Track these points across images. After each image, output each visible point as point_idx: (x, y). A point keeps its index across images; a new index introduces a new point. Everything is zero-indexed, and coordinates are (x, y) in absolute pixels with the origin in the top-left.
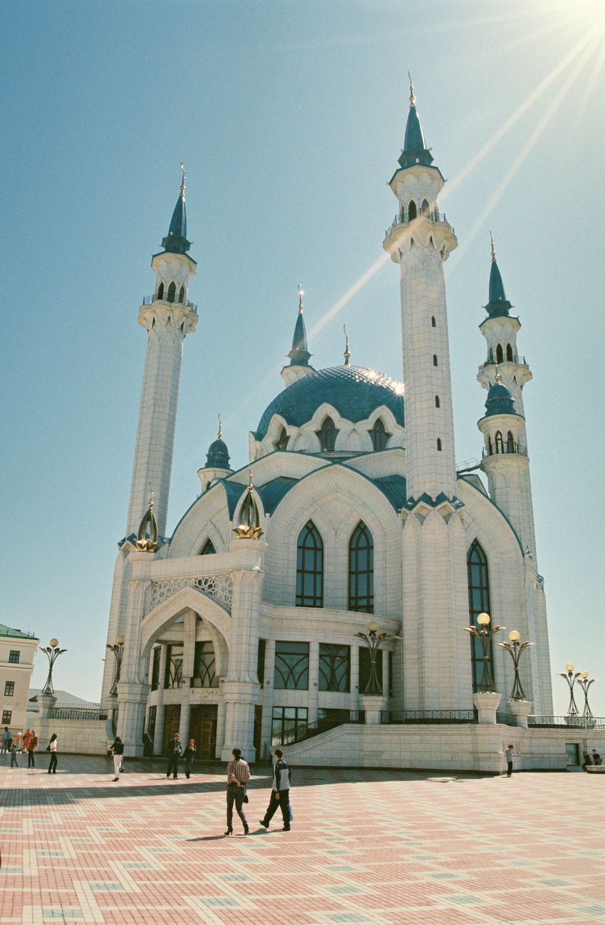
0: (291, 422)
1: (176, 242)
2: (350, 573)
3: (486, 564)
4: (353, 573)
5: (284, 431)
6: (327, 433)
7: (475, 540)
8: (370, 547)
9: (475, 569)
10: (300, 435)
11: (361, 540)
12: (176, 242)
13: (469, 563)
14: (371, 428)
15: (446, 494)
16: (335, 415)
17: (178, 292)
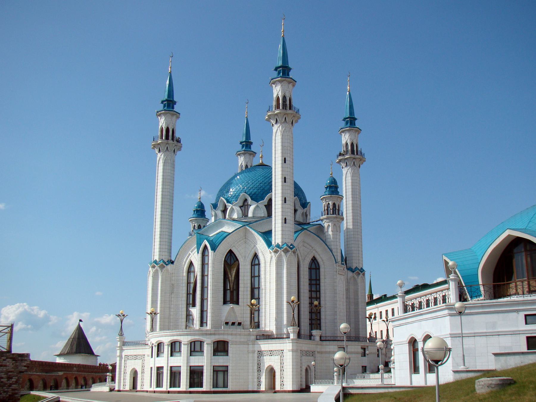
0: (228, 202)
1: (169, 104)
2: (252, 277)
3: (319, 269)
4: (253, 277)
5: (226, 206)
6: (244, 206)
7: (314, 257)
8: (259, 264)
9: (313, 271)
10: (232, 209)
11: (255, 260)
12: (169, 104)
13: (310, 269)
14: (266, 204)
16: (249, 199)
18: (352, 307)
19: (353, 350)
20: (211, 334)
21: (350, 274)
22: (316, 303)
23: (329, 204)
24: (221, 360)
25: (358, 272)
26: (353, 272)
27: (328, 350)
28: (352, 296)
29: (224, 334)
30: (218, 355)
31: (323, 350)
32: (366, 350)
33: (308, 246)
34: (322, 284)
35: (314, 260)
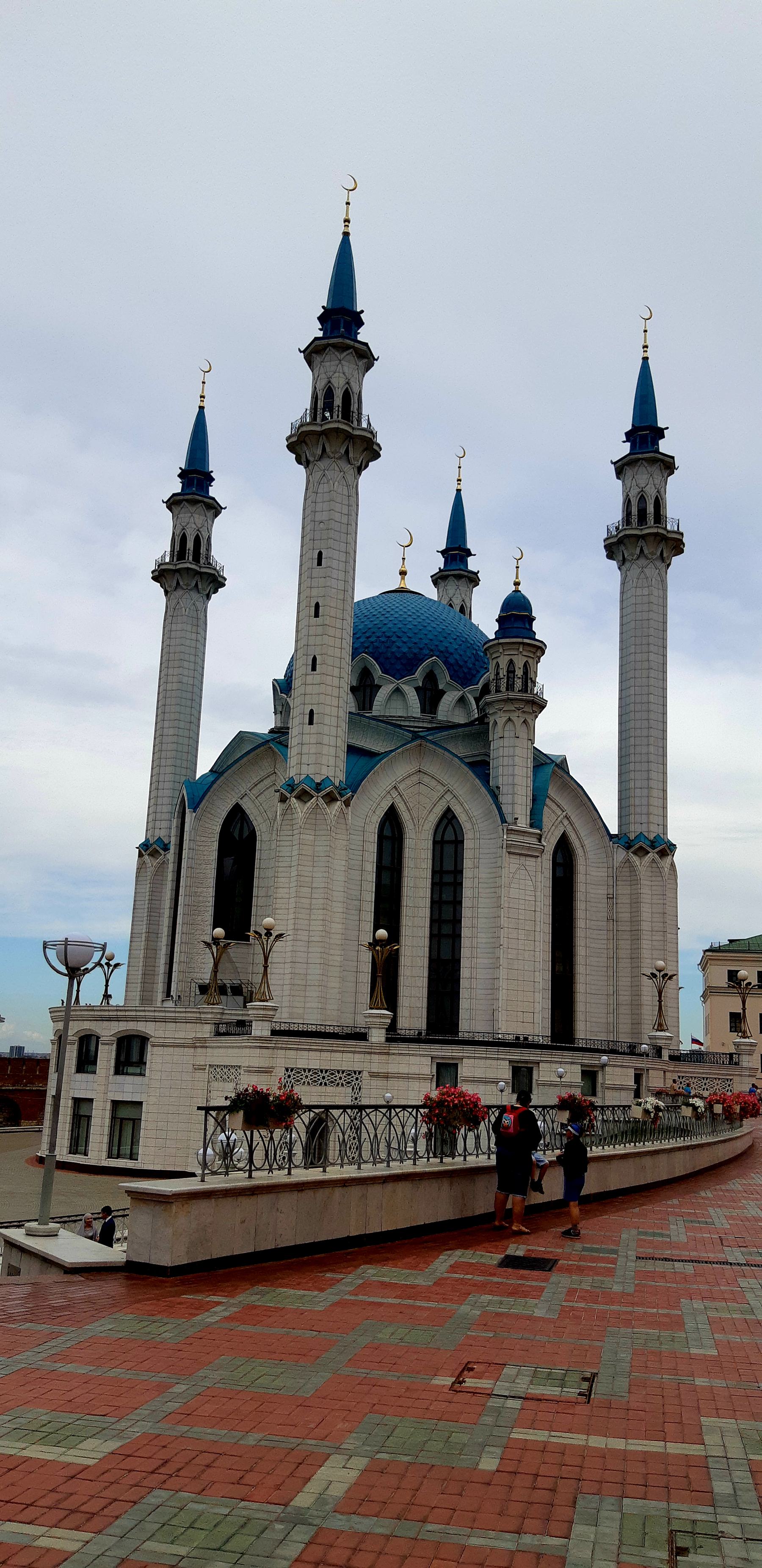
3: (462, 842)
15: (312, 776)
17: (190, 545)
18: (625, 945)
19: (479, 1073)
20: (109, 1019)
21: (621, 854)
22: (382, 933)
23: (498, 665)
24: (127, 1088)
25: (641, 848)
26: (628, 846)
27: (403, 1069)
28: (625, 916)
29: (135, 1019)
30: (127, 1074)
31: (392, 1068)
32: (535, 1073)
33: (433, 783)
34: (466, 883)
35: (448, 818)
